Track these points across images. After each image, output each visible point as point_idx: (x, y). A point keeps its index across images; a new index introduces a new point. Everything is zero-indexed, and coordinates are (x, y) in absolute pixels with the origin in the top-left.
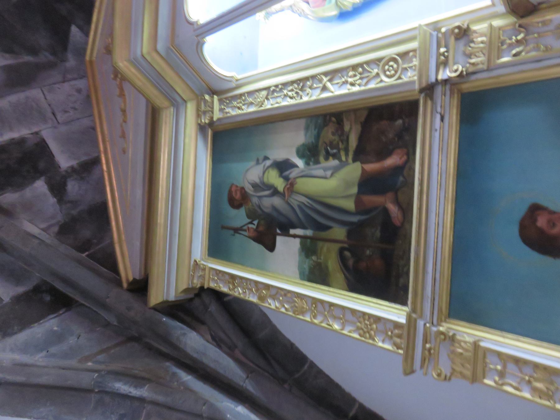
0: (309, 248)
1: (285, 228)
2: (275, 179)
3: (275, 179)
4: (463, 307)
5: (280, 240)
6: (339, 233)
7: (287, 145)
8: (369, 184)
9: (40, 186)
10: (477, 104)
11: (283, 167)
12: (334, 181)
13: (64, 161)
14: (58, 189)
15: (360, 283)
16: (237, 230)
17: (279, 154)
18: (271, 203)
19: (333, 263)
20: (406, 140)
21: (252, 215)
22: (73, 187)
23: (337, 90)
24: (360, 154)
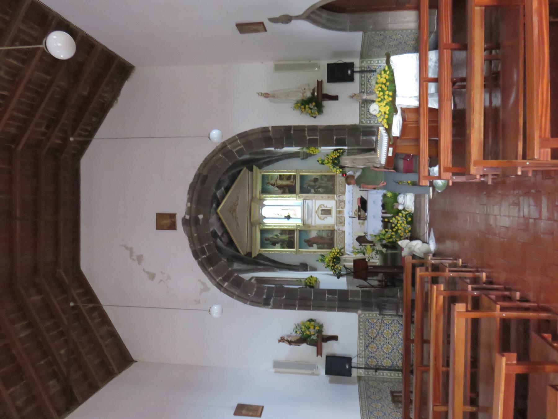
0: (281, 245)
1: (277, 243)
2: (275, 237)
3: (275, 237)
4: (300, 248)
5: (277, 245)
6: (286, 243)
7: (278, 233)
8: (289, 238)
9: (218, 240)
10: (300, 231)
11: (277, 235)
12: (285, 237)
13: (220, 234)
14: (221, 240)
15: (289, 247)
16: (267, 244)
17: (276, 234)
18: (274, 240)
19: (285, 246)
20: (294, 234)
21: (271, 242)
22: (223, 239)
23: (286, 228)
24: (289, 234)
